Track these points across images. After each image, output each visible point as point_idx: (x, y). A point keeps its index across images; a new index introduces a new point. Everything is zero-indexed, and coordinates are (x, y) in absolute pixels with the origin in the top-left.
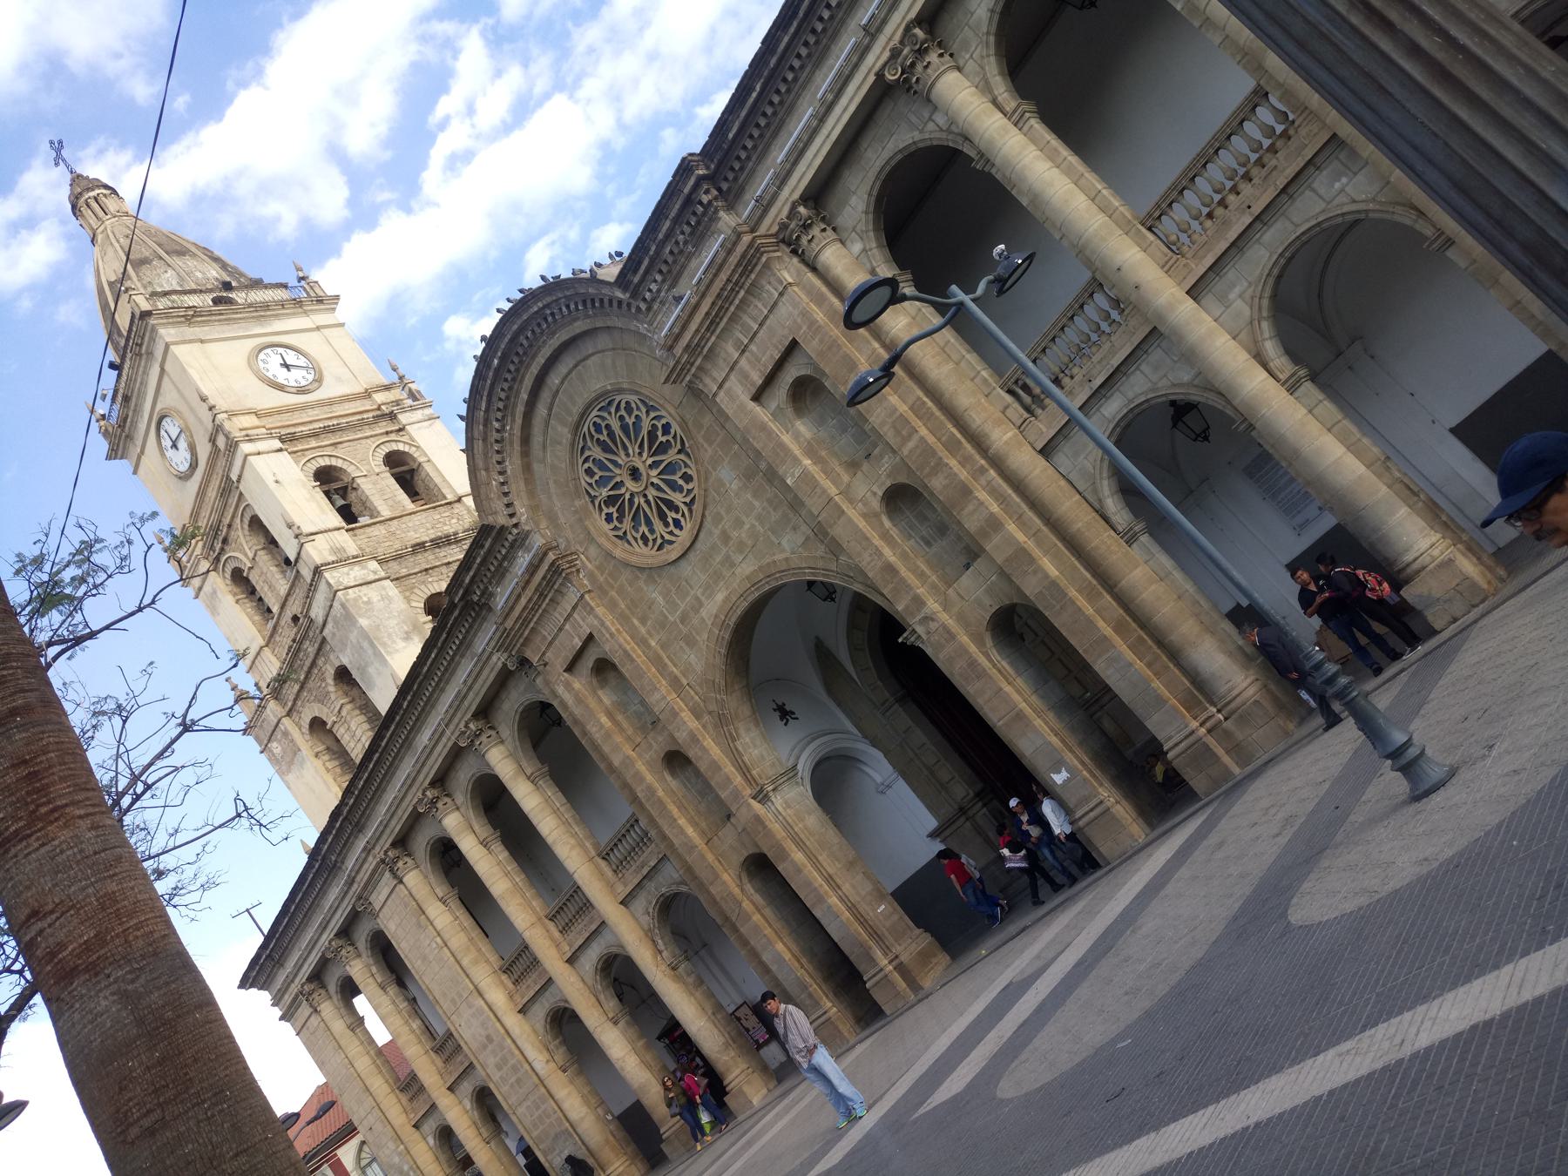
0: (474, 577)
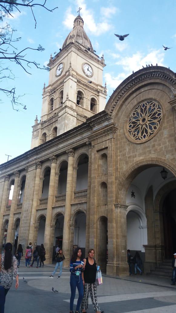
0: (94, 120)
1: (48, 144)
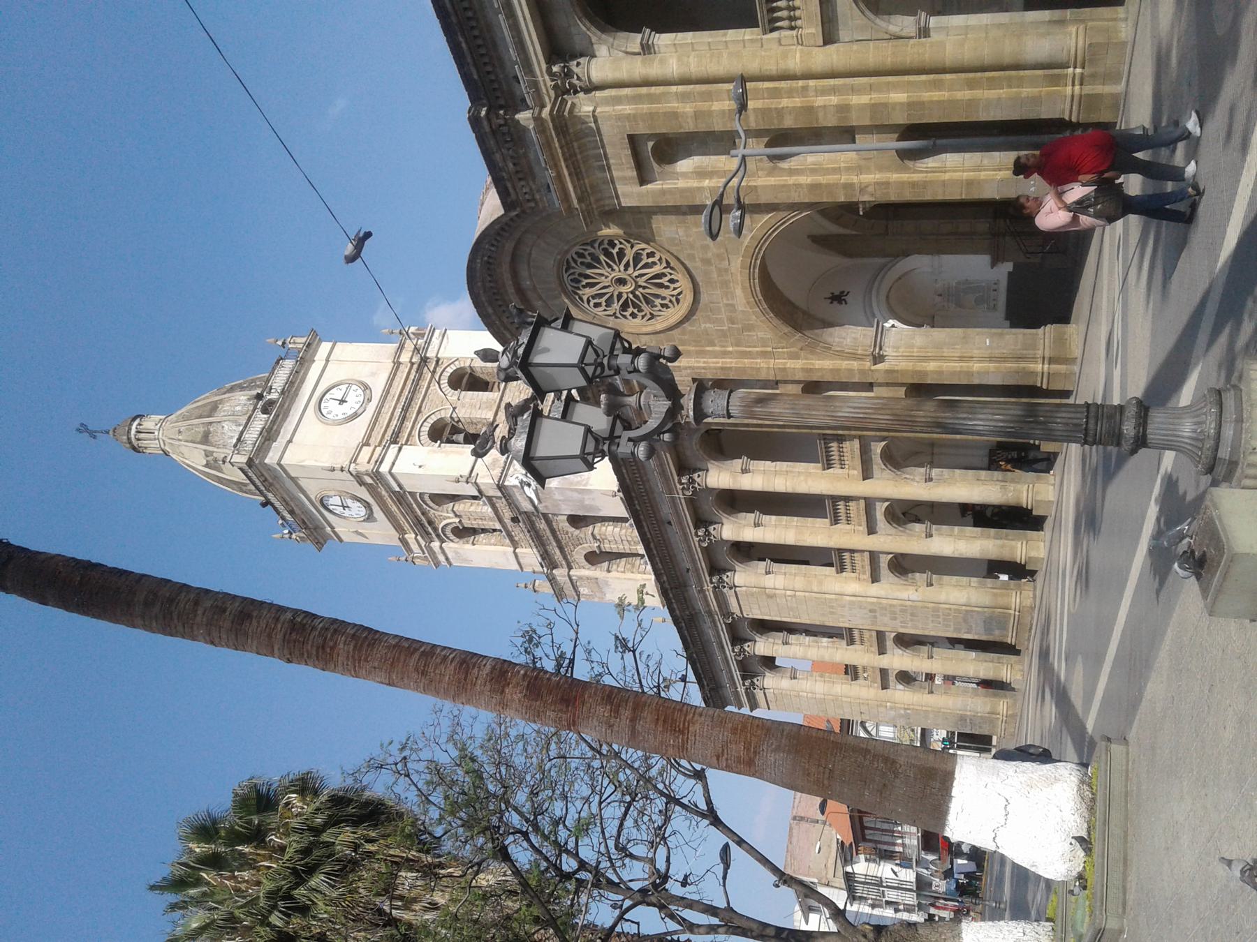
1: (655, 552)
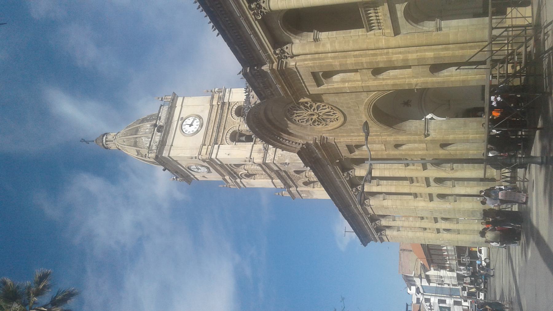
1: (335, 198)
